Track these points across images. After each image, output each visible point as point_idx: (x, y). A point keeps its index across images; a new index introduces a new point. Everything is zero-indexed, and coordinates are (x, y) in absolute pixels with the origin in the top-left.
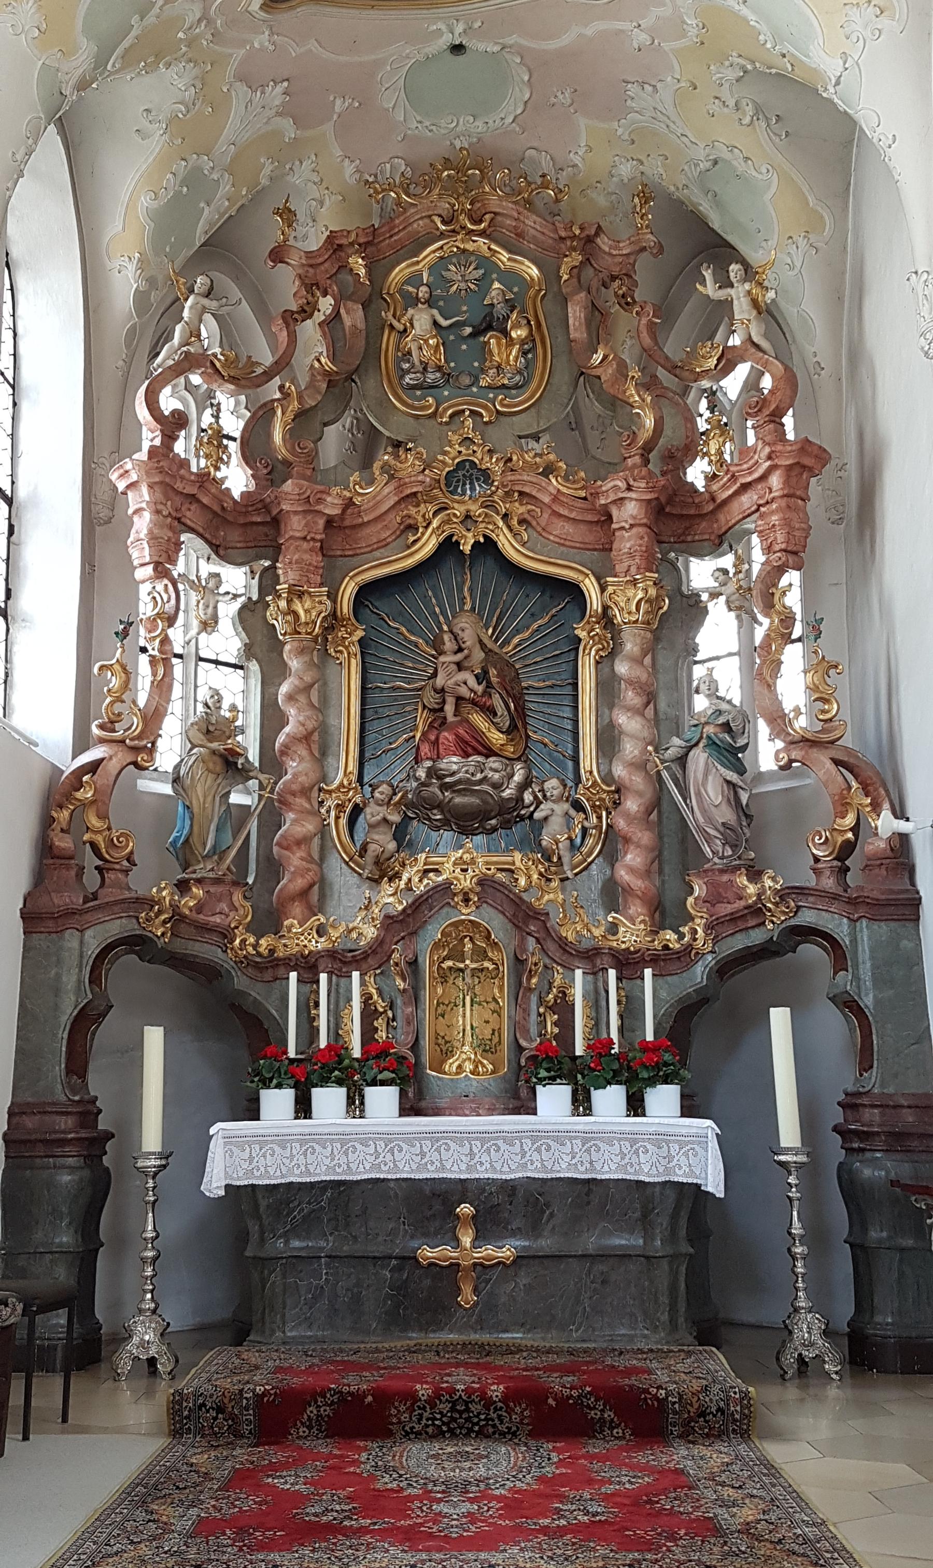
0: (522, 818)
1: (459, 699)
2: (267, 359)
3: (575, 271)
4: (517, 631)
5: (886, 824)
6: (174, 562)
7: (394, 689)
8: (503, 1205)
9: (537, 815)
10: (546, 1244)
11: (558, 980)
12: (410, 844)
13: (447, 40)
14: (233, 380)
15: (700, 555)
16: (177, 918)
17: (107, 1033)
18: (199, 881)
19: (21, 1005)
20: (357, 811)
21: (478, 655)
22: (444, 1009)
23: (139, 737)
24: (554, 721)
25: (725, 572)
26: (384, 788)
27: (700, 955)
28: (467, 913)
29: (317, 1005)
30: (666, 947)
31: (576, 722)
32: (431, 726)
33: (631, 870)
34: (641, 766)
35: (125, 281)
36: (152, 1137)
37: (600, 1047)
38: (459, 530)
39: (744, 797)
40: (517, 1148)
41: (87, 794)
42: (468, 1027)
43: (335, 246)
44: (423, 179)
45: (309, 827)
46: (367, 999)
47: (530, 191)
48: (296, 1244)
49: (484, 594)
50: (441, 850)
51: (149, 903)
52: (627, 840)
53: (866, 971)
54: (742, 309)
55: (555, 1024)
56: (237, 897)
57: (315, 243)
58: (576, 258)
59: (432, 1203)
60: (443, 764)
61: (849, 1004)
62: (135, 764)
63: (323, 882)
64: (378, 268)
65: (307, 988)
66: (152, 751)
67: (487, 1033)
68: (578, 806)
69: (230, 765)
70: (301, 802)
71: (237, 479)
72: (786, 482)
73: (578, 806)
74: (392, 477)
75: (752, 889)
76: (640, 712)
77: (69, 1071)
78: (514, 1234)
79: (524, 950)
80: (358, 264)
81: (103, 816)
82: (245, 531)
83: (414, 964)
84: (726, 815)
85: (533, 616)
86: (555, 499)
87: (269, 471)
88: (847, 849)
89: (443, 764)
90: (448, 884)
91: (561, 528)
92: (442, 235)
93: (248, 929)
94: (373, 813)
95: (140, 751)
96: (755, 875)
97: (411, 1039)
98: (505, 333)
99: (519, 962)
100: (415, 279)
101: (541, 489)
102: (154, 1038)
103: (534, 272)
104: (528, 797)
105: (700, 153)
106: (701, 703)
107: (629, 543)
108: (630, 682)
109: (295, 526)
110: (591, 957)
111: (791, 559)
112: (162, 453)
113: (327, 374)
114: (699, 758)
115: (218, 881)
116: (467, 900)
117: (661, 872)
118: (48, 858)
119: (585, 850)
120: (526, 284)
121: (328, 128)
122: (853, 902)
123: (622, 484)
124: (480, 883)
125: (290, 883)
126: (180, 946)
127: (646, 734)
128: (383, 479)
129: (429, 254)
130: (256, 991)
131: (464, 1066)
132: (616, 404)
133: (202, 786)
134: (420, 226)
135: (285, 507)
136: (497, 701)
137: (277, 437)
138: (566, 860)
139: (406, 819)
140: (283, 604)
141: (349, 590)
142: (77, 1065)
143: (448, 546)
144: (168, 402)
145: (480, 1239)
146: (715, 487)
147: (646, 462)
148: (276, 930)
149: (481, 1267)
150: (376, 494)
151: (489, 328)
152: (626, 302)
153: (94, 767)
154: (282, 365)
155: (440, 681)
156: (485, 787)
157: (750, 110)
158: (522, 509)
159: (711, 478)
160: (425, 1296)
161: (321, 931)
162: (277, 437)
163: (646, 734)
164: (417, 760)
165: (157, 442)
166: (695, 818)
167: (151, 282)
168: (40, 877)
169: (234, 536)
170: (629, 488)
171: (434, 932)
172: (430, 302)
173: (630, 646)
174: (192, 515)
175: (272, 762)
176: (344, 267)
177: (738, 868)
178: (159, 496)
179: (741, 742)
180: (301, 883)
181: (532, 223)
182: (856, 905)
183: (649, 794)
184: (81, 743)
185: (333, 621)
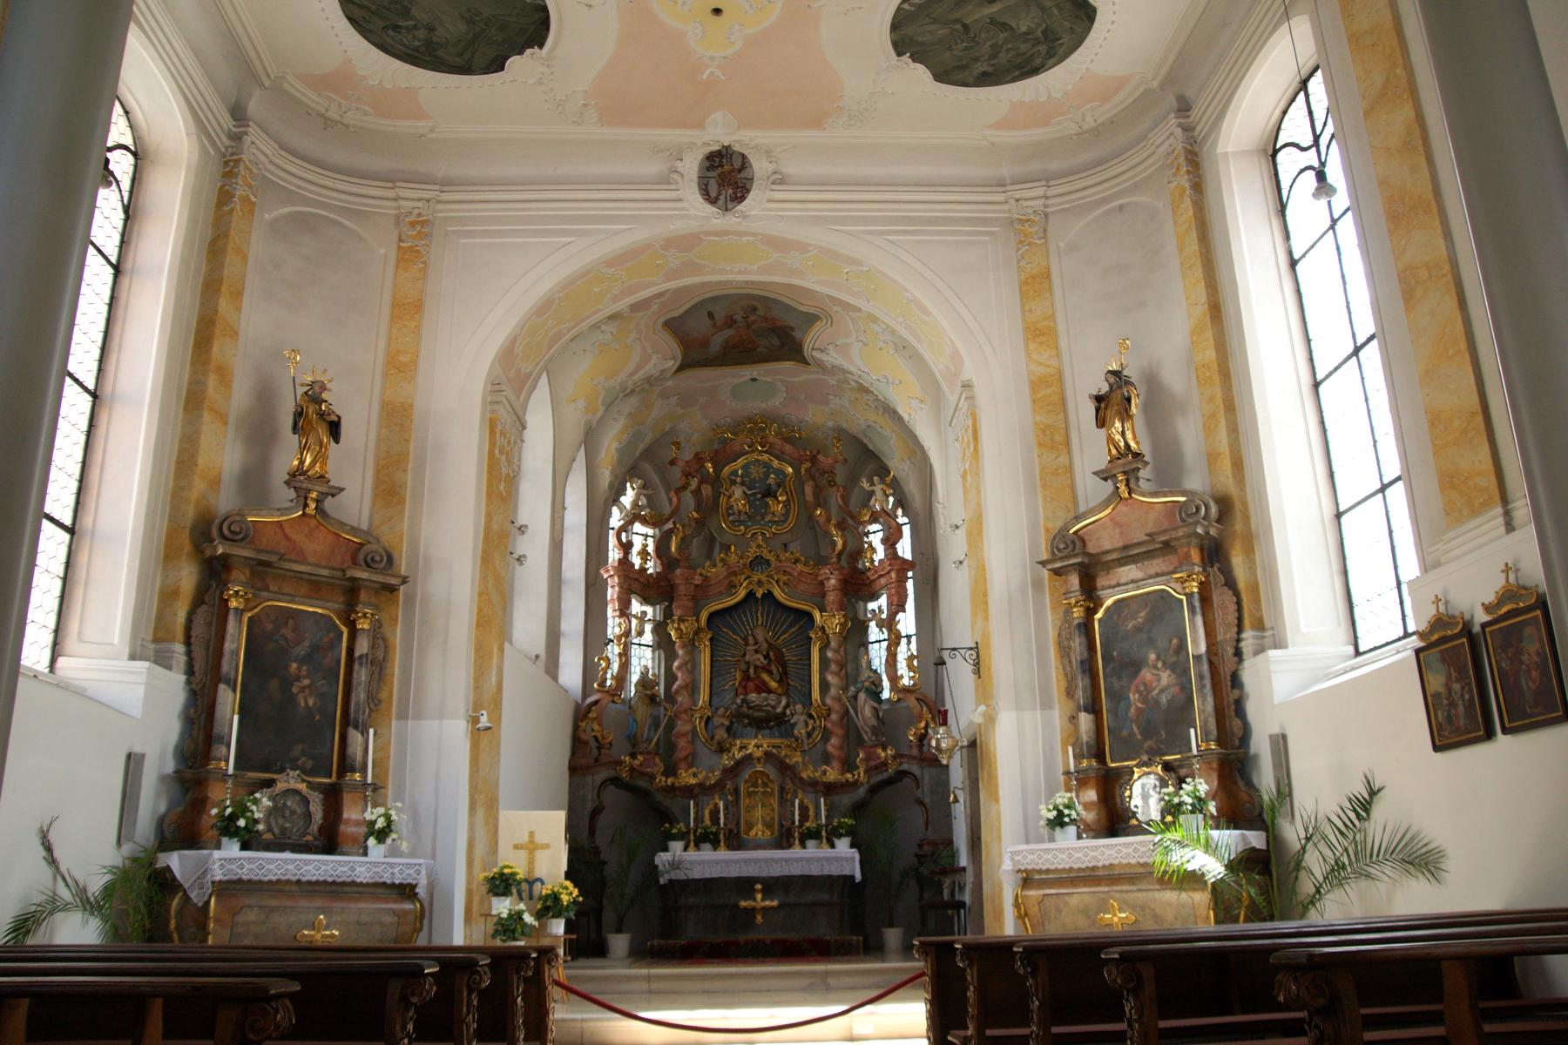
2: (667, 510)
8: (772, 885)
16: (632, 769)
21: (765, 646)
22: (749, 809)
35: (605, 477)
38: (756, 588)
41: (592, 715)
42: (759, 817)
43: (699, 458)
45: (687, 728)
51: (620, 763)
53: (926, 788)
56: (657, 760)
57: (688, 455)
58: (808, 465)
59: (745, 885)
64: (718, 468)
69: (653, 699)
70: (684, 716)
73: (811, 716)
76: (837, 674)
81: (600, 724)
83: (736, 791)
84: (873, 722)
85: (791, 626)
93: (664, 774)
94: (717, 720)
96: (884, 749)
99: (782, 789)
100: (735, 473)
107: (832, 597)
112: (625, 562)
114: (862, 696)
118: (577, 743)
120: (786, 475)
128: (720, 565)
129: (741, 461)
131: (759, 832)
133: (642, 712)
134: (737, 448)
141: (704, 615)
142: (592, 832)
143: (751, 595)
150: (716, 571)
152: (832, 483)
153: (596, 703)
161: (695, 775)
166: (860, 723)
172: (743, 484)
175: (670, 697)
176: (703, 466)
180: (684, 754)
181: (788, 448)
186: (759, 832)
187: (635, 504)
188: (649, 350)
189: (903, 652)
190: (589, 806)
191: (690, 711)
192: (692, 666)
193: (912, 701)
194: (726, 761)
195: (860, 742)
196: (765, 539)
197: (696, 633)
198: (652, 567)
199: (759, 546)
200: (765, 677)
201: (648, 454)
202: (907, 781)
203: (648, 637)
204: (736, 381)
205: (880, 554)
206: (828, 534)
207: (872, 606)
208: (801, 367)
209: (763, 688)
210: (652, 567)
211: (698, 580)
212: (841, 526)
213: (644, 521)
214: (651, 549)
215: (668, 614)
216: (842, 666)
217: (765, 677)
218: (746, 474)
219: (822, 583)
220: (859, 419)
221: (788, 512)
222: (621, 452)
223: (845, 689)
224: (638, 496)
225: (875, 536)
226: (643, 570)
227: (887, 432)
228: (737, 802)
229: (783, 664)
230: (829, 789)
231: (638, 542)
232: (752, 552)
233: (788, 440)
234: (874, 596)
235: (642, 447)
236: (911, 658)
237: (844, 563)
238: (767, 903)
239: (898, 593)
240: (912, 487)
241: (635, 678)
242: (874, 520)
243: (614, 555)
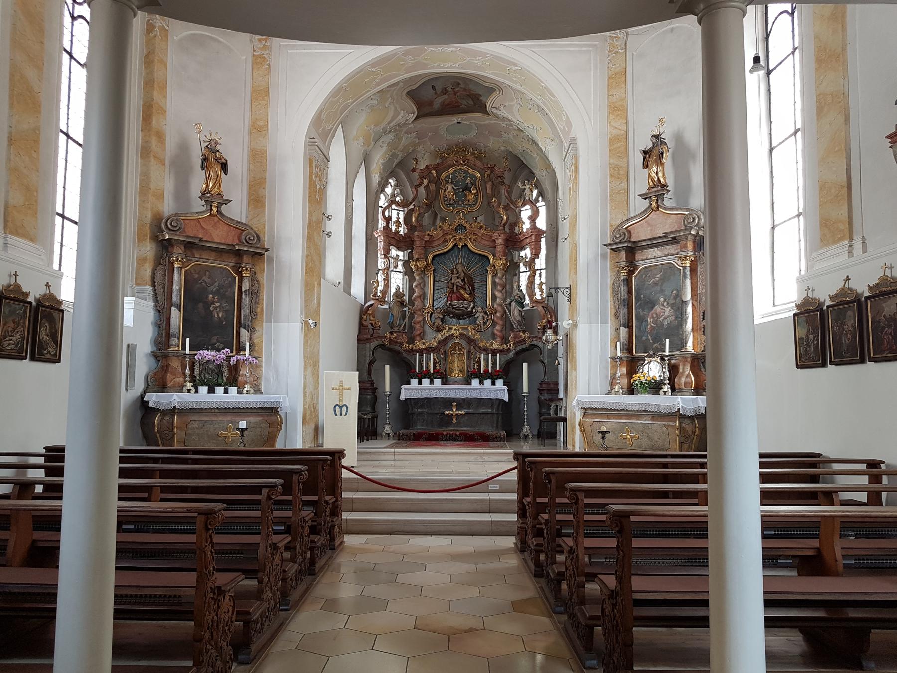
2: (411, 197)
3: (489, 176)
10: (471, 411)
17: (375, 366)
22: (452, 362)
28: (457, 341)
36: (388, 389)
37: (486, 371)
41: (370, 312)
42: (457, 366)
44: (450, 149)
45: (421, 318)
57: (423, 167)
59: (448, 403)
63: (424, 332)
64: (439, 174)
68: (486, 313)
69: (402, 303)
73: (486, 313)
76: (501, 291)
83: (445, 352)
84: (519, 318)
87: (411, 228)
91: (483, 242)
95: (382, 300)
96: (524, 333)
100: (448, 177)
102: (387, 367)
107: (499, 248)
110: (486, 350)
112: (387, 228)
114: (513, 304)
118: (362, 326)
121: (427, 139)
126: (391, 347)
129: (451, 170)
131: (456, 375)
133: (396, 310)
134: (450, 162)
142: (370, 373)
143: (455, 246)
148: (413, 343)
153: (372, 305)
161: (424, 344)
166: (512, 319)
167: (382, 179)
168: (360, 332)
169: (402, 244)
172: (452, 183)
175: (411, 302)
181: (478, 163)
186: (456, 375)
187: (393, 196)
189: (537, 281)
190: (368, 362)
193: (540, 308)
194: (439, 337)
195: (512, 328)
196: (464, 215)
197: (425, 267)
198: (402, 230)
199: (460, 219)
200: (462, 291)
204: (448, 123)
205: (527, 226)
206: (498, 213)
207: (523, 253)
209: (461, 298)
210: (402, 230)
211: (427, 238)
212: (506, 208)
213: (397, 204)
214: (401, 220)
215: (410, 256)
216: (504, 287)
217: (462, 291)
218: (455, 177)
219: (494, 241)
220: (519, 146)
221: (477, 199)
222: (385, 165)
223: (504, 300)
224: (394, 190)
225: (526, 213)
226: (397, 232)
230: (494, 352)
231: (394, 219)
232: (457, 222)
233: (479, 158)
234: (523, 248)
235: (396, 161)
236: (541, 283)
237: (507, 229)
239: (535, 248)
240: (547, 186)
241: (393, 290)
242: (524, 205)
243: (381, 224)
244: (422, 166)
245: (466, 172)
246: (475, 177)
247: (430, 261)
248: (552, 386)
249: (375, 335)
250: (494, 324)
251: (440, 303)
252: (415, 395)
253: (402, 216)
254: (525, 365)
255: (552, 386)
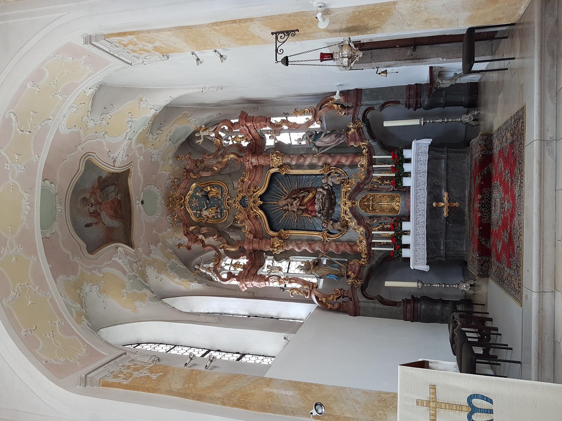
0: (332, 189)
1: (300, 205)
2: (214, 252)
4: (283, 190)
5: (337, 97)
6: (265, 276)
7: (297, 222)
8: (433, 195)
9: (331, 185)
10: (444, 184)
11: (375, 180)
12: (338, 218)
13: (140, 205)
14: (219, 260)
15: (265, 143)
16: (356, 278)
17: (386, 297)
18: (347, 272)
19: (378, 317)
20: (329, 232)
22: (382, 210)
23: (310, 286)
24: (306, 181)
25: (270, 137)
26: (323, 225)
27: (369, 144)
28: (358, 203)
29: (380, 243)
30: (367, 152)
31: (307, 175)
32: (307, 213)
33: (347, 161)
34: (319, 158)
35: (195, 286)
36: (414, 285)
37: (393, 170)
38: (257, 204)
39: (328, 132)
40: (419, 191)
42: (387, 203)
43: (187, 234)
44: (171, 212)
45: (333, 244)
46: (379, 230)
47: (175, 185)
48: (442, 248)
49: (273, 198)
50: (340, 210)
51: (352, 285)
52: (339, 162)
53: (374, 102)
54: (206, 133)
55: (387, 181)
56: (351, 263)
58: (191, 174)
59: (433, 213)
60: (317, 210)
61: (383, 106)
62: (317, 287)
63: (348, 242)
64: (192, 223)
65: (376, 245)
66: (313, 283)
67: (389, 199)
68: (329, 175)
69: (317, 264)
70: (326, 246)
71: (243, 261)
72: (249, 122)
73: (329, 175)
74: (243, 221)
75: (352, 130)
76: (305, 159)
77: (395, 306)
78: (441, 192)
79: (367, 189)
80: (191, 228)
81: (330, 296)
82: (256, 260)
83: (370, 217)
84: (333, 137)
86: (250, 180)
88: (343, 106)
89: (317, 210)
90: (350, 208)
91: (257, 178)
92: (185, 207)
94: (330, 228)
95: (313, 286)
96: (349, 129)
97: (390, 218)
98: (209, 192)
99: (371, 190)
100: (195, 214)
101: (247, 183)
102: (388, 284)
103: (194, 184)
104: (326, 188)
105: (168, 143)
106: (304, 143)
107: (262, 161)
108: (297, 161)
109: (256, 246)
110: (369, 171)
111: (268, 120)
113: (218, 237)
114: (318, 143)
115: (347, 268)
116: (354, 203)
117: (347, 153)
118: (340, 310)
119: (341, 173)
121: (160, 235)
122: (357, 105)
123: (247, 163)
124: (350, 200)
125: (348, 250)
127: (311, 157)
129: (189, 211)
130: (376, 259)
131: (397, 205)
132: (227, 164)
133: (323, 271)
134: (182, 213)
135: (251, 248)
136: (301, 195)
137: (233, 250)
138: (343, 178)
139: (331, 219)
140: (275, 249)
141: (271, 233)
142: (394, 304)
143: (261, 207)
144: (225, 276)
145: (442, 201)
146: (249, 139)
147: (242, 157)
149: (449, 201)
150: (247, 226)
151: (207, 196)
152: (202, 162)
153: (317, 298)
154: (215, 248)
155: (295, 210)
156: (324, 199)
157: (159, 131)
158: (252, 188)
159: (247, 140)
160: (456, 215)
161: (361, 242)
162: (233, 250)
163: (311, 157)
164: (316, 216)
165: (235, 279)
166: (333, 144)
167: (195, 279)
169: (258, 262)
170: (248, 161)
171: (362, 212)
172: (201, 211)
173: (288, 161)
174: (253, 272)
176: (192, 232)
177: (347, 134)
178: (248, 279)
179: (314, 133)
180: (348, 247)
181: (182, 185)
182: (357, 105)
183: (327, 156)
184: (311, 301)
185: (280, 237)
188: (109, 262)
191: (323, 242)
192: (299, 241)
194: (353, 224)
198: (243, 261)
199: (235, 202)
201: (187, 262)
202: (369, 116)
203: (284, 264)
208: (132, 174)
209: (312, 201)
211: (251, 236)
215: (270, 253)
217: (306, 200)
226: (244, 267)
227: (173, 129)
228: (378, 217)
229: (300, 190)
230: (371, 162)
232: (238, 206)
235: (180, 265)
238: (445, 199)
239: (259, 122)
244: (185, 240)
245: (192, 196)
246: (196, 188)
247: (275, 234)
248: (412, 92)
249: (350, 295)
250: (339, 166)
251: (318, 222)
252: (423, 253)
253: (229, 261)
254: (386, 124)
255: (412, 92)
